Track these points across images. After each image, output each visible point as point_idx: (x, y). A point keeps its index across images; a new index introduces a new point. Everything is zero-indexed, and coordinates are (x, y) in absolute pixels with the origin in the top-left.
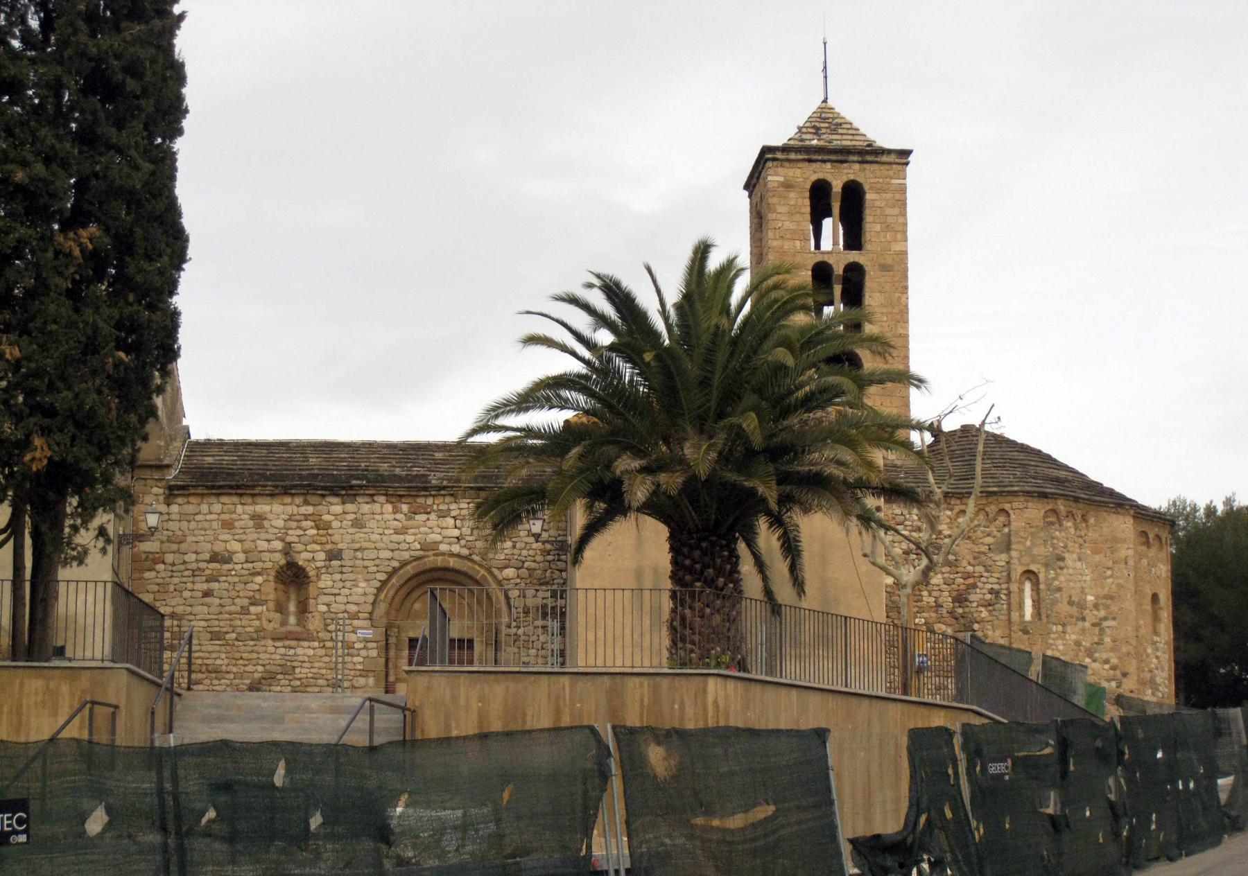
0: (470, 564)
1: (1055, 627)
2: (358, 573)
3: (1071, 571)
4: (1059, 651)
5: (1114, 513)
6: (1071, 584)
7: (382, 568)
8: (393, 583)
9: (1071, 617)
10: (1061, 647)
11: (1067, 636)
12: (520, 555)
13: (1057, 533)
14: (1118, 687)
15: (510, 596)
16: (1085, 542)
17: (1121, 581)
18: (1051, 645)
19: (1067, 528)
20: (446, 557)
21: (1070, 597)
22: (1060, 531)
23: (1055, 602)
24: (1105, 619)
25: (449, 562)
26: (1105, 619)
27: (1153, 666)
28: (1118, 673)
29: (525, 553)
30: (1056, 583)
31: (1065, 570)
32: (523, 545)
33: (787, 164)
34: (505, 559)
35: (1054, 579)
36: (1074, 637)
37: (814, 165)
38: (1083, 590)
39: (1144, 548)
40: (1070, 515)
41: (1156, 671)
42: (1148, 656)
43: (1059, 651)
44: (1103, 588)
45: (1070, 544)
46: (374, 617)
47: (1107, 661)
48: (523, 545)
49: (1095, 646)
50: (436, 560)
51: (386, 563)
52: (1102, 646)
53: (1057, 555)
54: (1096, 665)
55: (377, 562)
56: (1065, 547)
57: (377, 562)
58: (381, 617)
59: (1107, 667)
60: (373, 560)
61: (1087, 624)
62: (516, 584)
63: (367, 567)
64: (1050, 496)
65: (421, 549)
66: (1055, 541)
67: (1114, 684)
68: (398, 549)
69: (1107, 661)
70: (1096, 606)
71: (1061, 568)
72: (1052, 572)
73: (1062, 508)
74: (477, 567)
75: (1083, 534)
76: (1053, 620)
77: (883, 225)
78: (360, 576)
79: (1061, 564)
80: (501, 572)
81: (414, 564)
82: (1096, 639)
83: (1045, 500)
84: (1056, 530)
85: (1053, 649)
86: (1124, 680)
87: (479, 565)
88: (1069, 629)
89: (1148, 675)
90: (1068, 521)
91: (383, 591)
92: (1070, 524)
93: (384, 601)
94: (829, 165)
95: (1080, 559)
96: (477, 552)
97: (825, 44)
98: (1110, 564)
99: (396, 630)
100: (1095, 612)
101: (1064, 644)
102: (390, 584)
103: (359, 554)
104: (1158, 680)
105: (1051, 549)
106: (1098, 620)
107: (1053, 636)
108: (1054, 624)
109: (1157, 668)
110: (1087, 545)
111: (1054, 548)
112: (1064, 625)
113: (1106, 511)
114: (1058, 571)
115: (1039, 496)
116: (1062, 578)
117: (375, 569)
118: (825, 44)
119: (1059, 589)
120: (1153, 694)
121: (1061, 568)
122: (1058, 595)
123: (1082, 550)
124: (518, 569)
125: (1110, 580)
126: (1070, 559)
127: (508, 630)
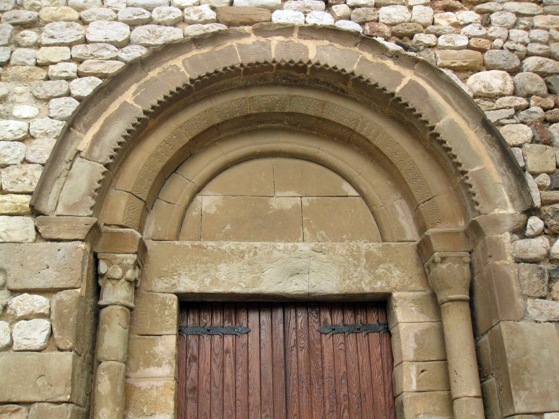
0: (369, 56)
2: (18, 79)
7: (97, 67)
8: (125, 104)
12: (508, 39)
15: (510, 139)
20: (295, 38)
25: (306, 49)
29: (518, 34)
32: (512, 18)
34: (468, 47)
46: (47, 205)
48: (512, 18)
50: (264, 44)
51: (106, 54)
55: (78, 51)
57: (78, 51)
58: (75, 206)
60: (70, 45)
62: (518, 110)
63: (44, 66)
65: (217, 21)
68: (150, 21)
74: (390, 63)
78: (19, 89)
80: (464, 80)
81: (195, 52)
87: (395, 56)
91: (87, 127)
93: (89, 157)
96: (387, 30)
99: (131, 259)
102: (114, 107)
103: (30, 36)
117: (72, 68)
124: (513, 72)
127: (522, 243)
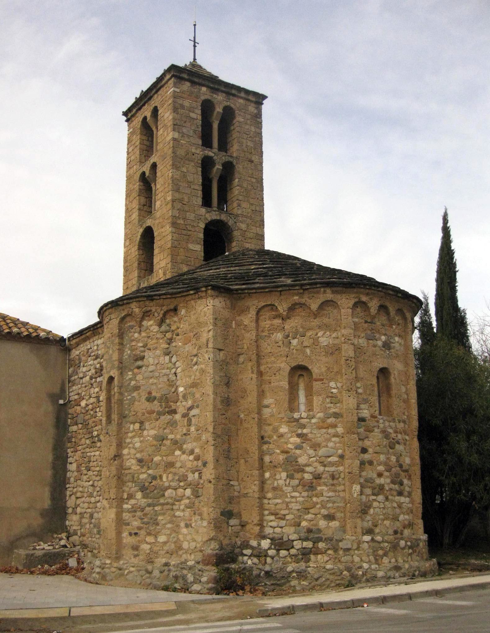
1: (132, 426)
3: (151, 368)
4: (136, 449)
5: (199, 298)
6: (151, 381)
9: (152, 412)
10: (138, 445)
11: (145, 433)
13: (136, 335)
14: (200, 477)
16: (178, 335)
17: (203, 366)
18: (129, 443)
19: (147, 328)
21: (150, 393)
22: (140, 332)
23: (133, 400)
24: (190, 409)
26: (190, 409)
27: (290, 446)
28: (200, 463)
30: (133, 383)
31: (144, 368)
33: (133, 119)
35: (131, 379)
36: (153, 432)
37: (142, 110)
38: (172, 384)
39: (278, 321)
40: (146, 314)
41: (298, 452)
42: (281, 436)
43: (136, 449)
44: (190, 376)
45: (151, 343)
47: (192, 452)
49: (184, 437)
52: (189, 437)
53: (135, 355)
54: (184, 457)
56: (145, 346)
59: (191, 457)
61: (178, 417)
64: (121, 303)
66: (134, 343)
67: (197, 475)
69: (192, 452)
70: (185, 397)
71: (139, 367)
72: (130, 373)
73: (137, 310)
75: (173, 328)
76: (131, 419)
77: (164, 128)
79: (139, 363)
82: (185, 431)
83: (121, 308)
84: (135, 332)
85: (130, 448)
86: (205, 469)
88: (147, 425)
89: (281, 457)
90: (149, 320)
92: (151, 322)
94: (146, 105)
95: (167, 353)
97: (195, 25)
98: (195, 352)
100: (184, 403)
101: (141, 442)
104: (302, 460)
105: (129, 352)
106: (186, 411)
107: (130, 435)
108: (131, 423)
109: (299, 447)
110: (180, 337)
111: (132, 350)
112: (142, 423)
113: (192, 299)
114: (136, 371)
115: (111, 308)
116: (139, 377)
118: (195, 25)
119: (137, 388)
120: (291, 477)
121: (139, 367)
122: (135, 394)
123: (174, 344)
125: (196, 367)
126: (150, 358)
